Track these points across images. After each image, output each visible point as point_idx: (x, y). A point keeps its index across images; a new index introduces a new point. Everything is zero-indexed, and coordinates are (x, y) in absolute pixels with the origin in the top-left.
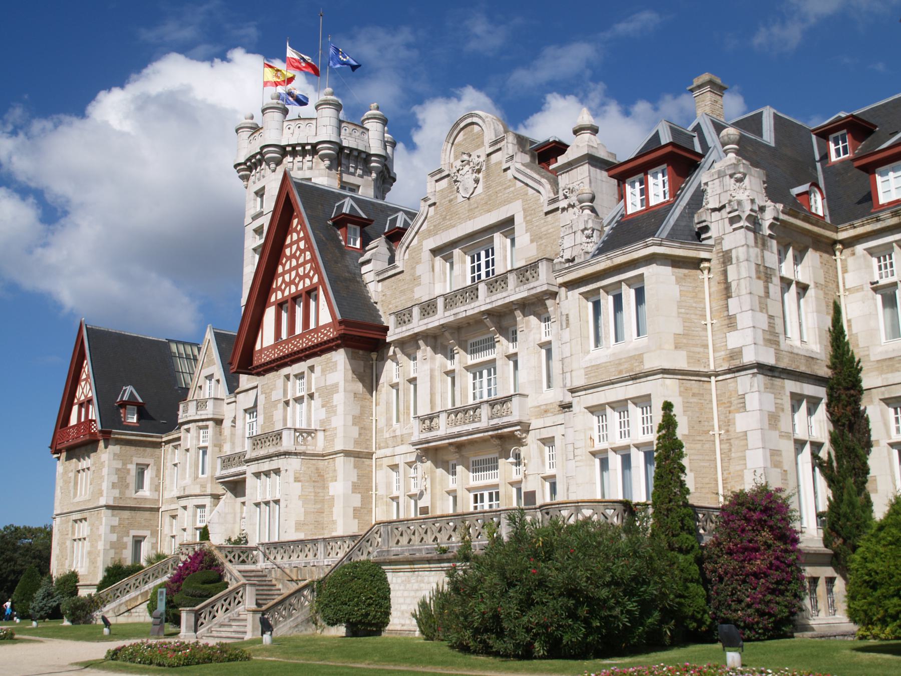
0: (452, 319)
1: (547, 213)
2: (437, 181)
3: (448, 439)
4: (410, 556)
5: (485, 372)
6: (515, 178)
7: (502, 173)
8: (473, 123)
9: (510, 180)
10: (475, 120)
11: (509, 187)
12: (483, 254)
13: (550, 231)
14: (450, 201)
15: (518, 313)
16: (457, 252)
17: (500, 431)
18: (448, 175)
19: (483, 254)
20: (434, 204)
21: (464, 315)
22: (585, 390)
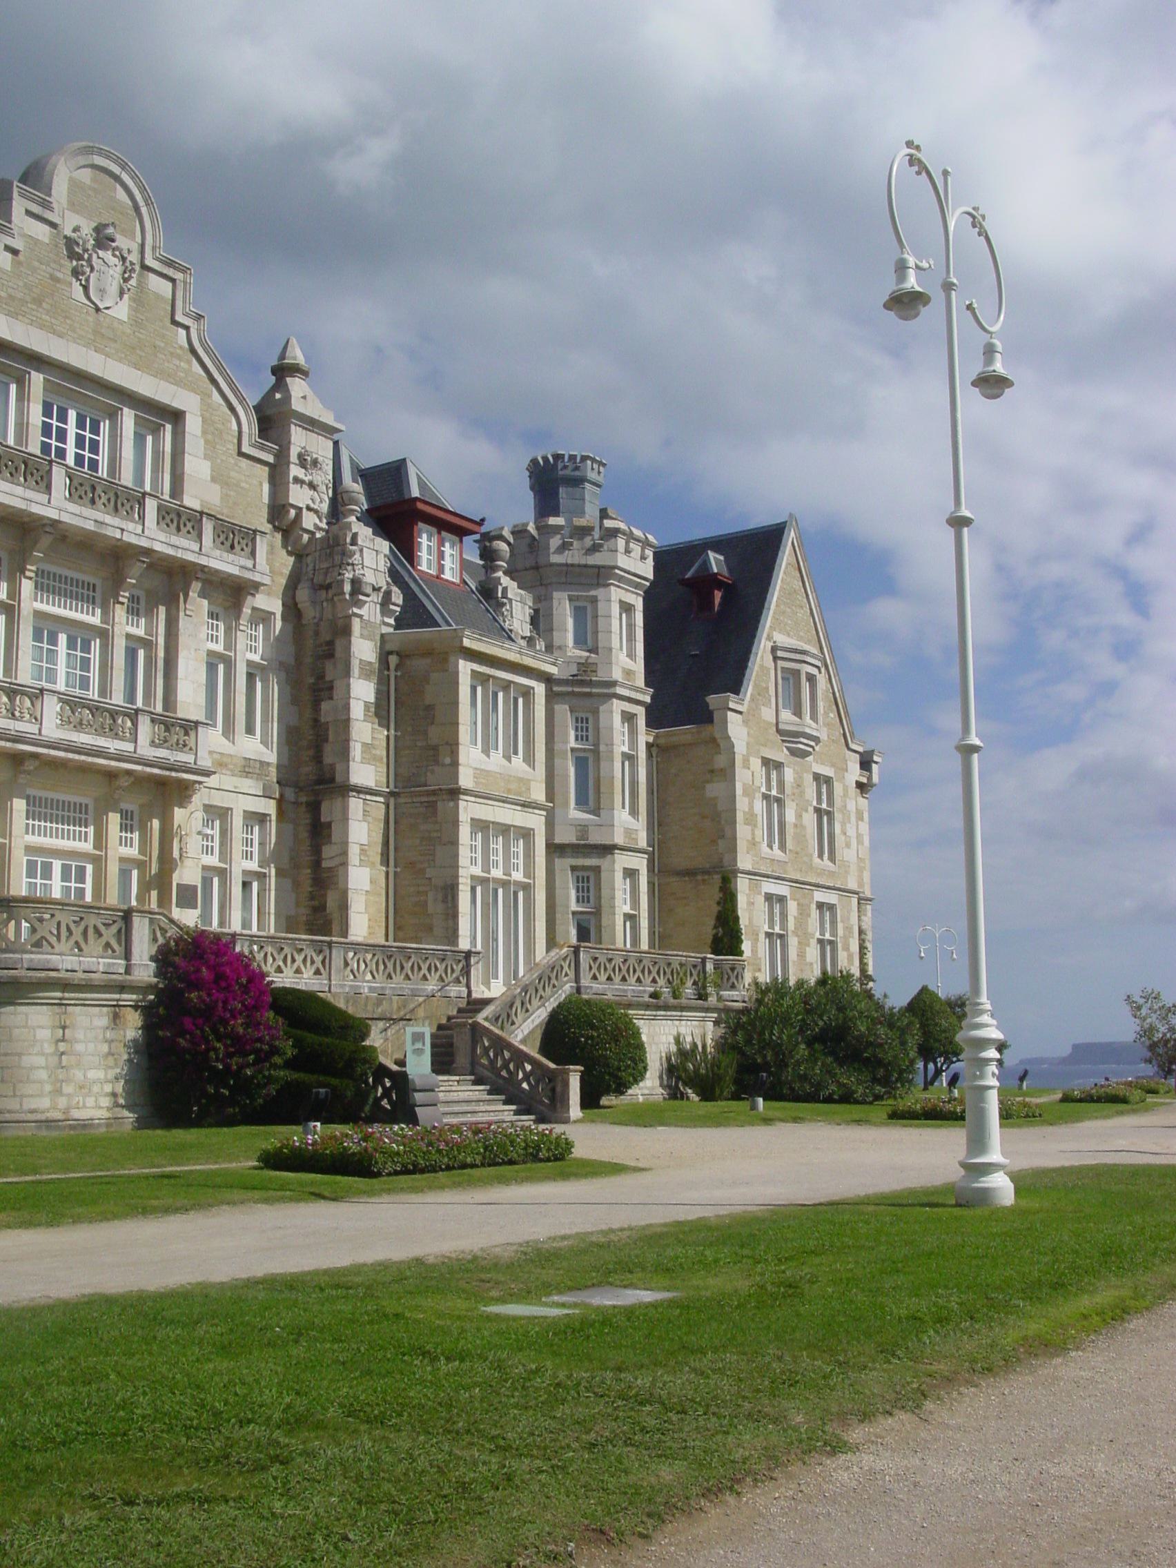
0: (90, 526)
1: (241, 454)
2: (29, 213)
3: (66, 750)
4: (613, 998)
5: (63, 639)
6: (193, 351)
7: (168, 321)
8: (117, 178)
9: (181, 347)
10: (125, 177)
11: (179, 358)
12: (72, 415)
13: (243, 485)
14: (53, 278)
15: (196, 586)
16: (37, 379)
17: (174, 774)
18: (53, 225)
19: (72, 415)
20: (15, 252)
21: (118, 536)
22: (476, 796)
